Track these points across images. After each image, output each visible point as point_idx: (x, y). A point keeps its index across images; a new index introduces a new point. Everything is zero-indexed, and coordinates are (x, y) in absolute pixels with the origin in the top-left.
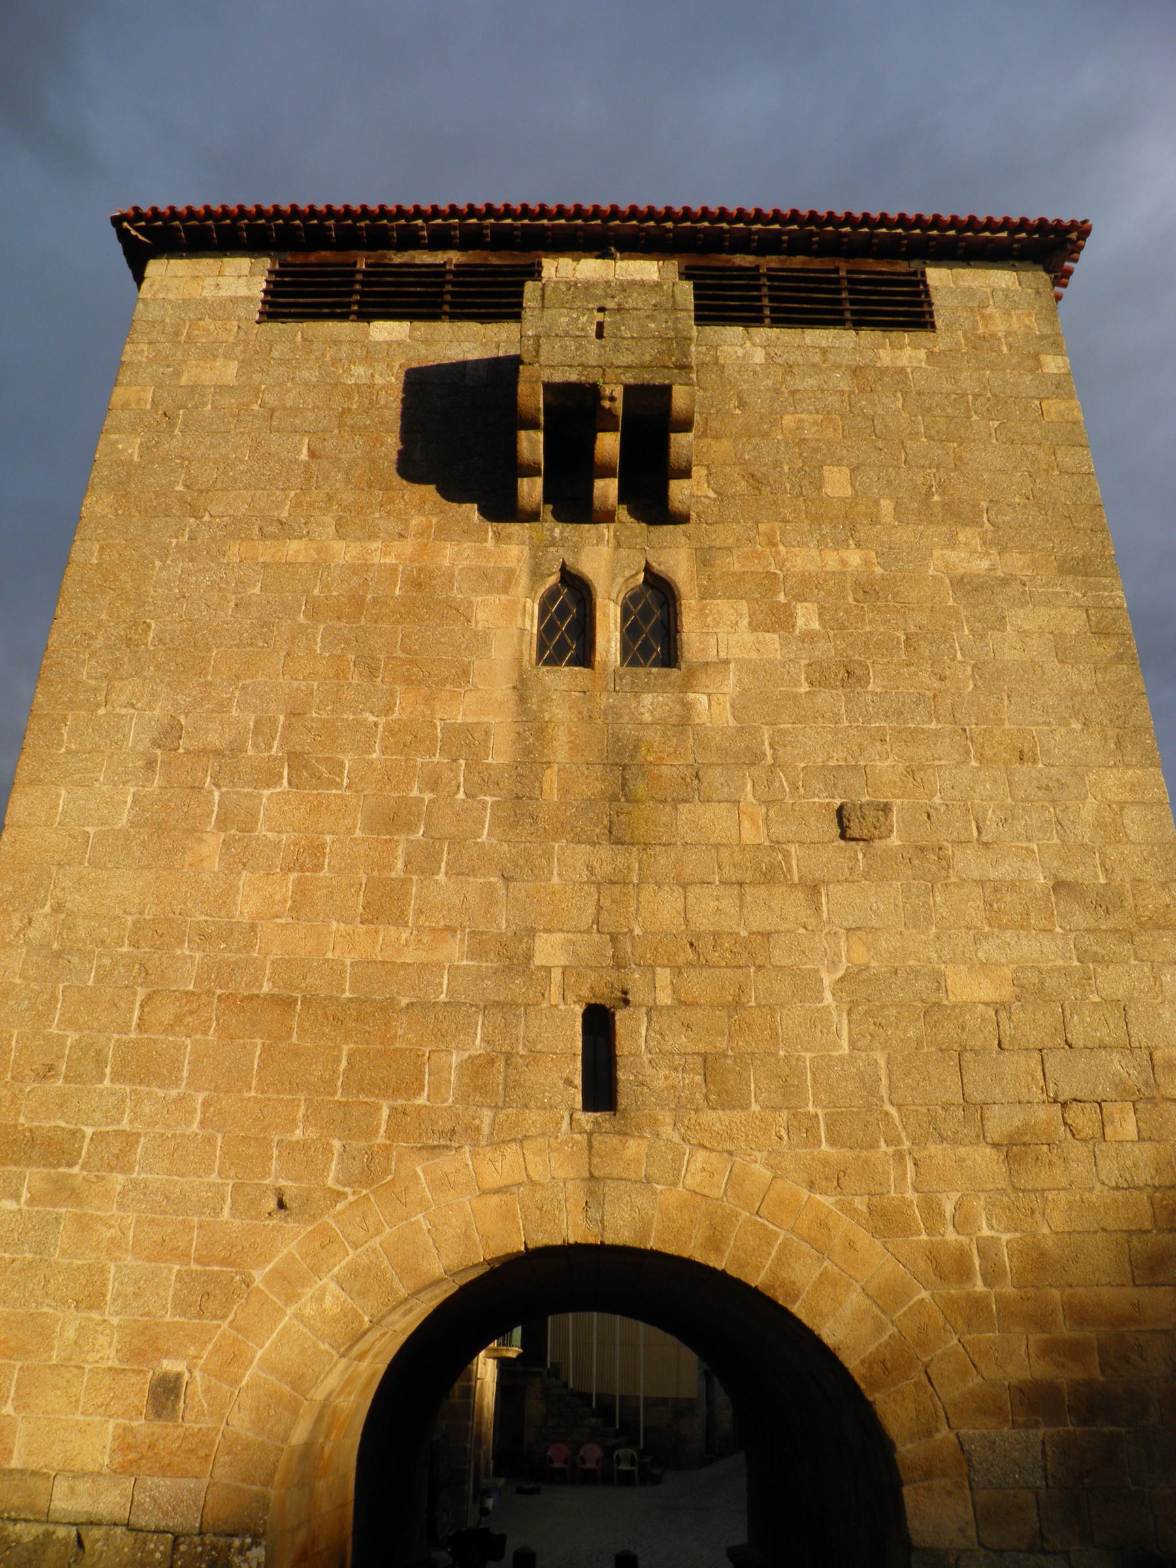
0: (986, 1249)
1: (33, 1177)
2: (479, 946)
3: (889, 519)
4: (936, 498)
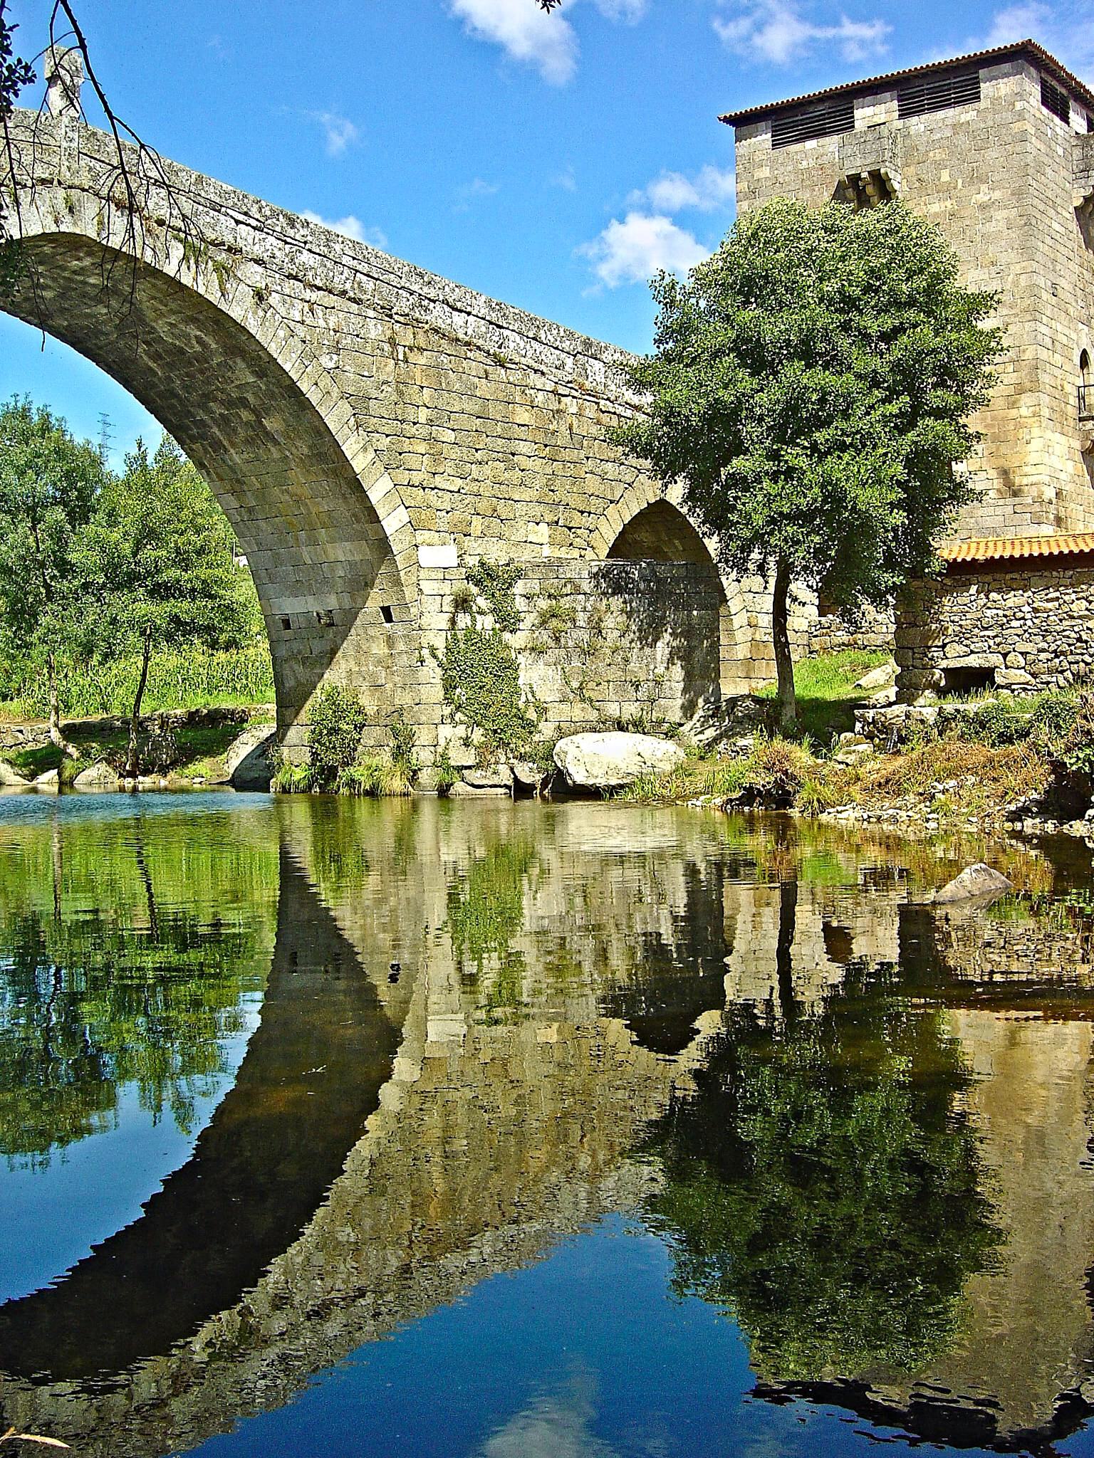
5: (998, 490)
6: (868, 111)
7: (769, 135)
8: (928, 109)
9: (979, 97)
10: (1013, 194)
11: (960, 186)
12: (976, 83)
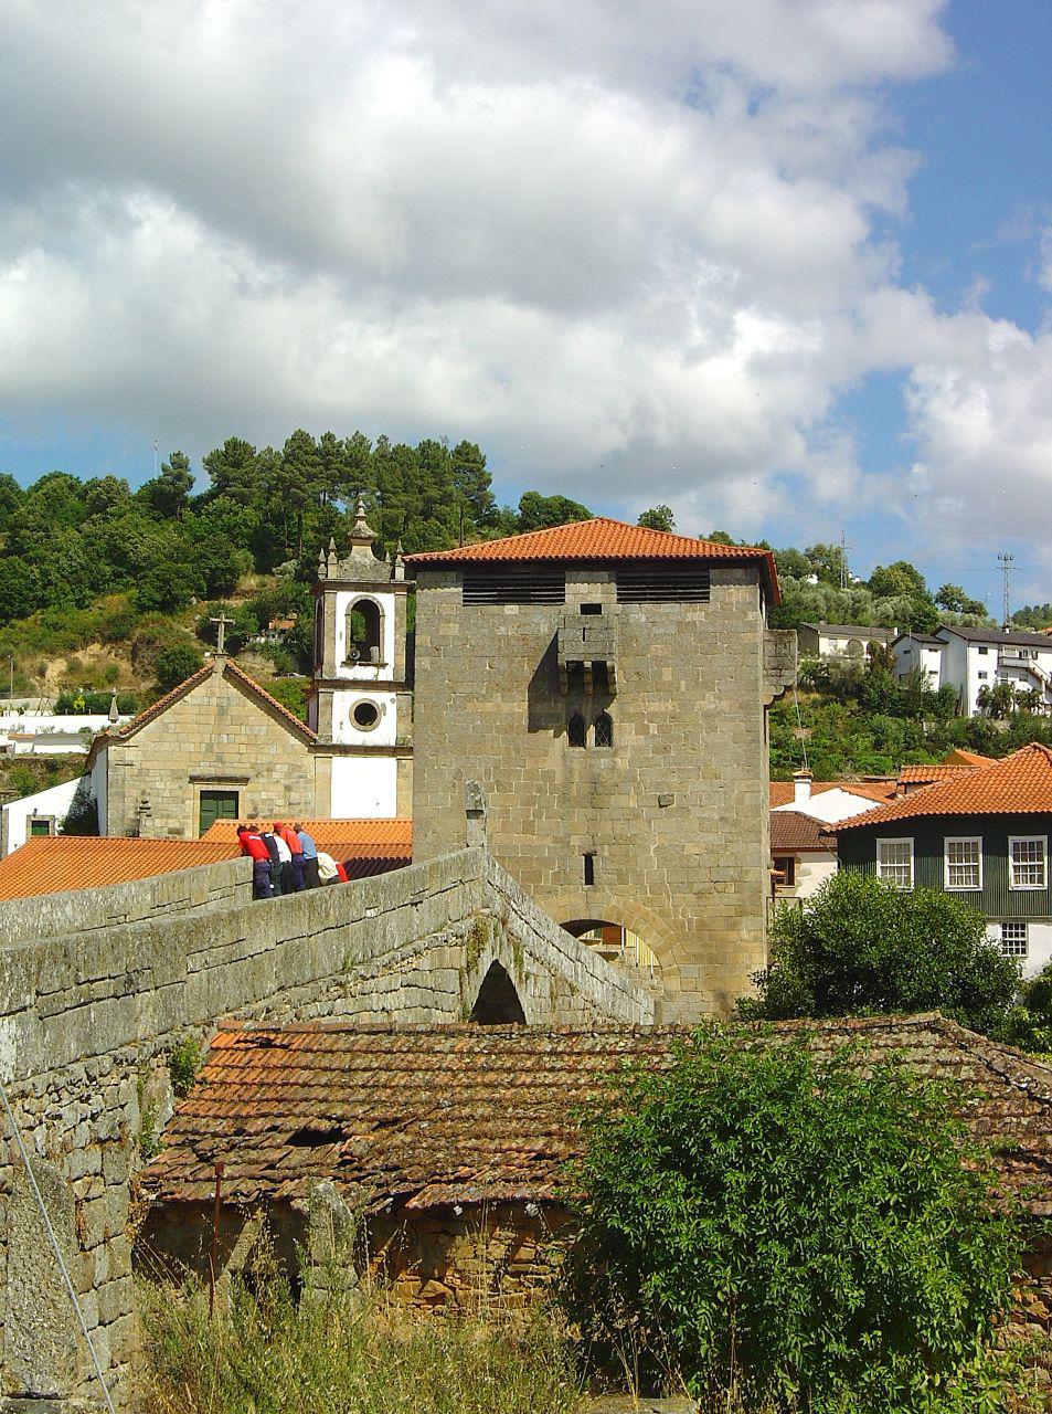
0: (690, 921)
2: (555, 840)
3: (683, 689)
7: (461, 589)
8: (650, 599)
9: (708, 598)
10: (741, 707)
11: (683, 689)
12: (706, 583)
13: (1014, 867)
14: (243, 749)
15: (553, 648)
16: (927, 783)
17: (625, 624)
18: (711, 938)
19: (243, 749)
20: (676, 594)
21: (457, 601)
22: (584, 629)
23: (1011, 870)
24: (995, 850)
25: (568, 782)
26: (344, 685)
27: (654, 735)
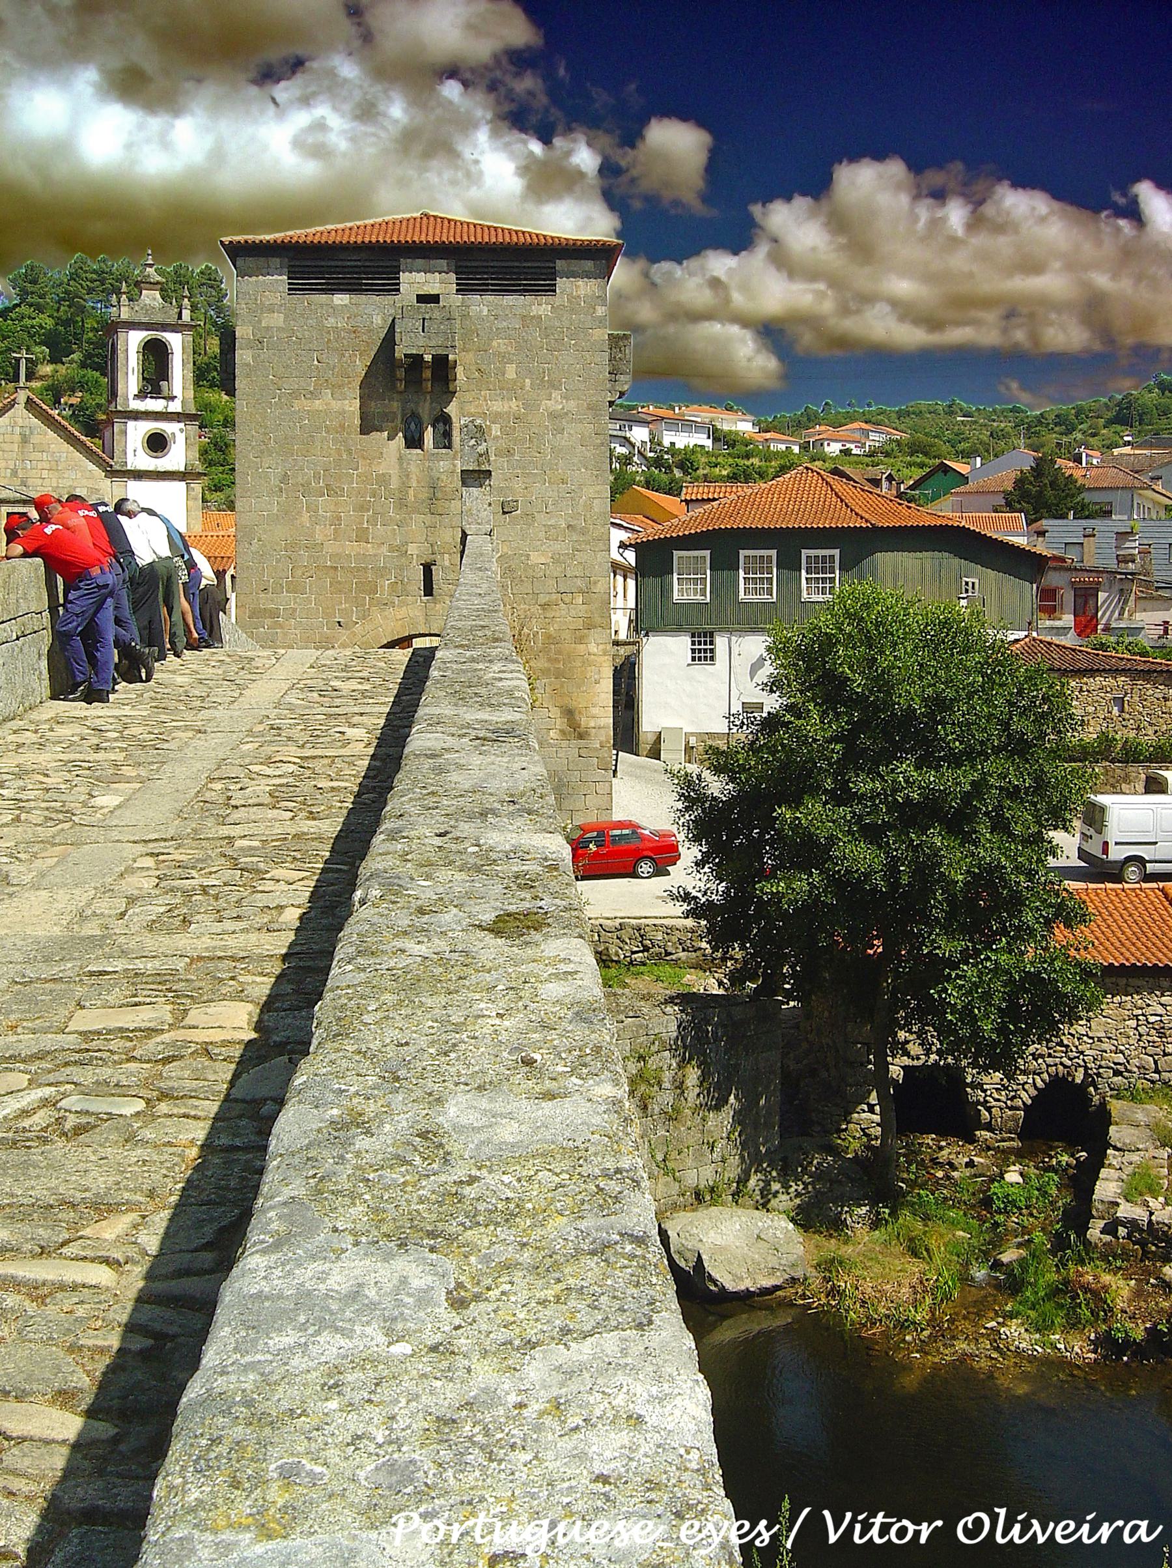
1: (268, 621)
4: (546, 378)
5: (562, 732)
6: (420, 277)
7: (286, 277)
9: (554, 291)
12: (553, 275)
13: (745, 578)
14: (45, 474)
15: (389, 341)
16: (714, 500)
17: (465, 316)
18: (559, 652)
19: (45, 474)
20: (520, 285)
21: (281, 289)
22: (424, 319)
23: (804, 581)
24: (789, 563)
25: (404, 487)
26: (137, 416)
27: (496, 438)
